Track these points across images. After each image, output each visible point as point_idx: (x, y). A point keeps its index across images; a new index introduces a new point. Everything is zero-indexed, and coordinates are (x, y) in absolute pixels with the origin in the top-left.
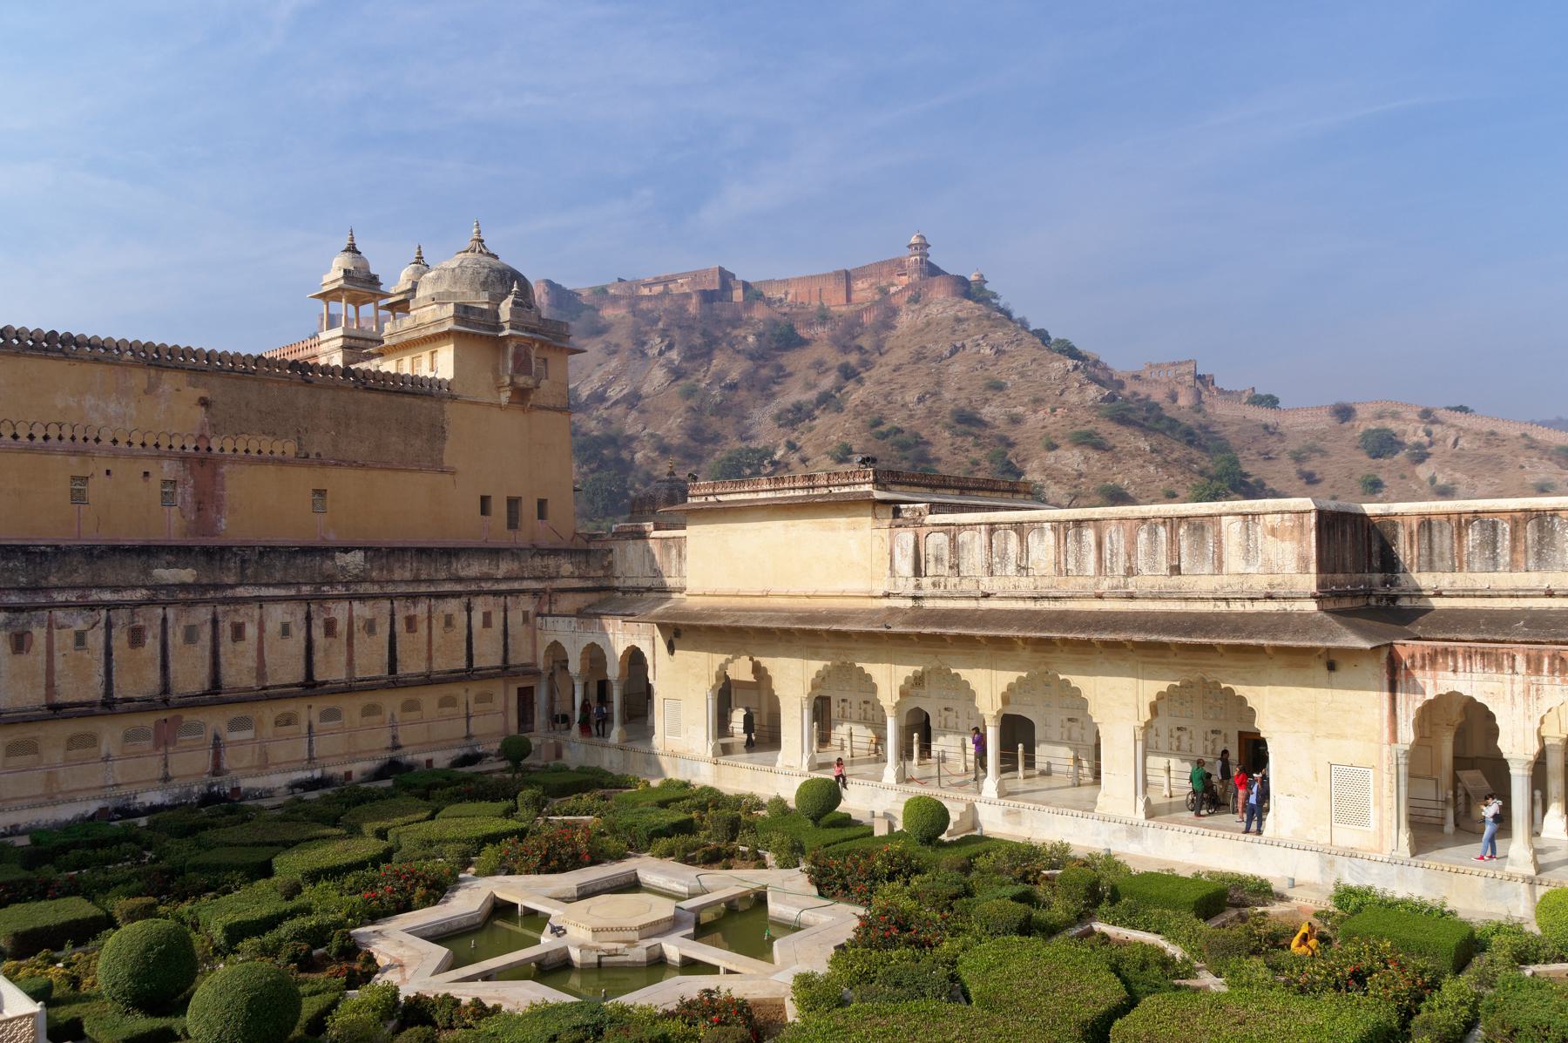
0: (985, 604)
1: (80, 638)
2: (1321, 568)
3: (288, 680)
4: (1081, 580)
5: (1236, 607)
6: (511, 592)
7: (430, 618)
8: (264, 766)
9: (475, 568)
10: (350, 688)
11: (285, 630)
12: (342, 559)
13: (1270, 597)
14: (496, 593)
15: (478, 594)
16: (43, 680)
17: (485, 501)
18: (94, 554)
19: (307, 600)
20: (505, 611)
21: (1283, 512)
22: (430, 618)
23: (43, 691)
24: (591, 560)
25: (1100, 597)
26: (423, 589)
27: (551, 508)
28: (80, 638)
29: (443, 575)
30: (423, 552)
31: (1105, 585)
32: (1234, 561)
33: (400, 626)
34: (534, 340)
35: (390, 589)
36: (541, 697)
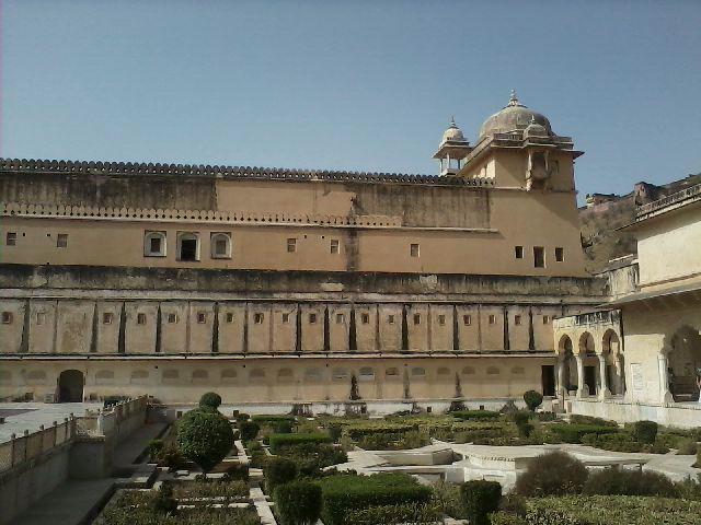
1: (285, 317)
3: (393, 347)
8: (380, 398)
9: (511, 288)
10: (429, 358)
11: (391, 319)
12: (427, 279)
14: (522, 305)
15: (512, 304)
16: (267, 337)
17: (519, 251)
18: (292, 275)
19: (404, 304)
20: (531, 315)
22: (479, 318)
23: (268, 344)
24: (593, 285)
26: (474, 299)
28: (285, 317)
29: (488, 291)
30: (474, 278)
33: (461, 320)
35: (453, 299)
36: (560, 373)
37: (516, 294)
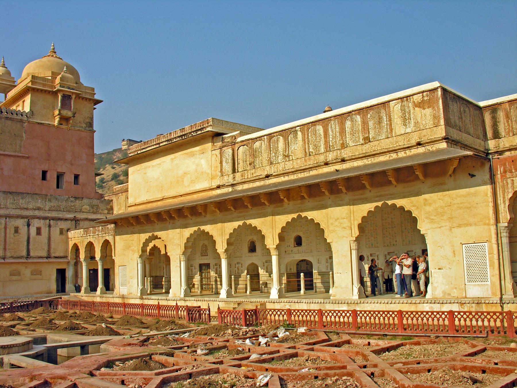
0: (268, 182)
2: (448, 123)
4: (317, 157)
5: (402, 154)
6: (54, 219)
7: (5, 228)
13: (419, 144)
14: (45, 218)
20: (50, 226)
21: (423, 92)
22: (5, 228)
25: (326, 164)
27: (81, 179)
31: (331, 157)
32: (399, 129)
34: (73, 93)
37: (39, 209)
